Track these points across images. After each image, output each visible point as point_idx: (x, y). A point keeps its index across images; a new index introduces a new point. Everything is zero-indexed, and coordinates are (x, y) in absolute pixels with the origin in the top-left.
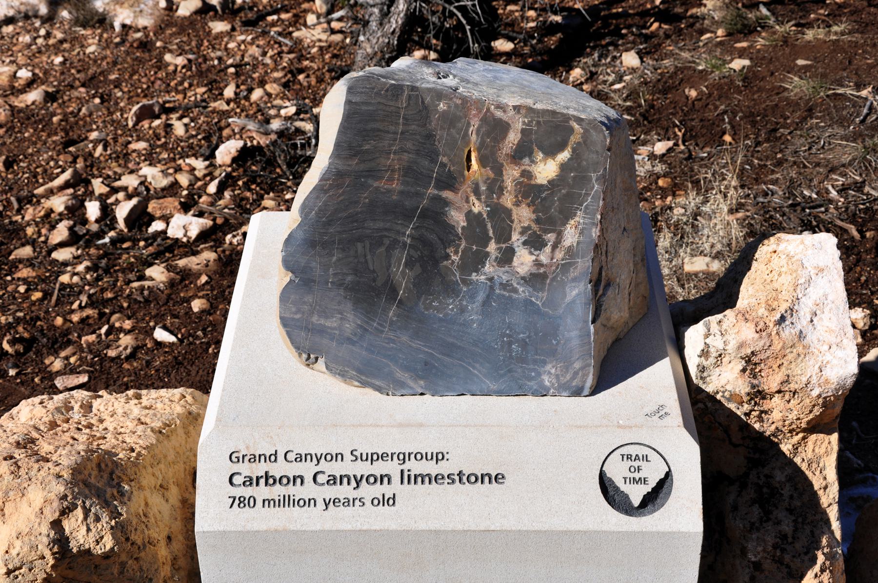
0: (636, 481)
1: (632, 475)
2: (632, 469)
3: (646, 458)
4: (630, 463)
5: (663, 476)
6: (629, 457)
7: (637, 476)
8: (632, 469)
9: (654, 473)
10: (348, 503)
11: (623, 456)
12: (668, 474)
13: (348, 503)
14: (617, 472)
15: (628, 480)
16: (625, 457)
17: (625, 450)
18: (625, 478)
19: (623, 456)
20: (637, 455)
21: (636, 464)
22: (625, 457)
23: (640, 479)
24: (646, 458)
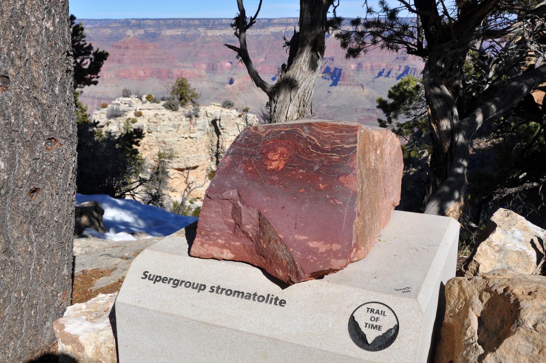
0: (373, 327)
1: (371, 323)
2: (373, 319)
3: (383, 313)
4: (372, 314)
5: (392, 327)
6: (372, 311)
7: (375, 323)
8: (373, 319)
9: (387, 323)
12: (397, 328)
14: (362, 319)
15: (368, 325)
16: (370, 310)
18: (366, 324)
19: (368, 309)
21: (376, 316)
22: (370, 310)
23: (376, 326)
24: (383, 313)
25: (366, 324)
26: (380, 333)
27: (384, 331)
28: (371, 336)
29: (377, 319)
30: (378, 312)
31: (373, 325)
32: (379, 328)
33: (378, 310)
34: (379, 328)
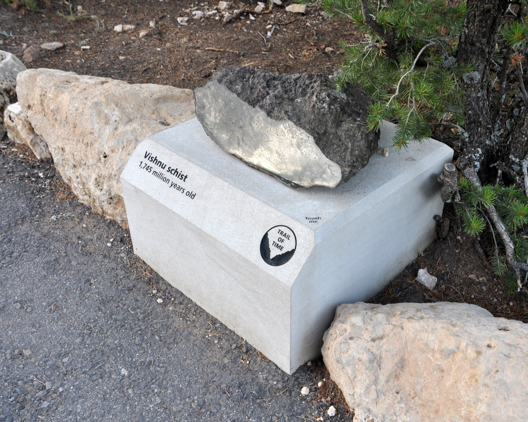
0: (278, 246)
1: (278, 242)
2: (280, 240)
3: (288, 237)
4: (281, 236)
6: (282, 233)
7: (280, 244)
9: (288, 246)
10: (179, 188)
11: (280, 230)
13: (179, 188)
14: (273, 237)
17: (283, 229)
18: (274, 242)
19: (280, 230)
20: (286, 234)
21: (283, 238)
25: (274, 242)
26: (280, 253)
27: (284, 251)
28: (274, 252)
29: (282, 241)
30: (285, 235)
31: (278, 245)
32: (281, 248)
33: (286, 234)
34: (281, 248)
